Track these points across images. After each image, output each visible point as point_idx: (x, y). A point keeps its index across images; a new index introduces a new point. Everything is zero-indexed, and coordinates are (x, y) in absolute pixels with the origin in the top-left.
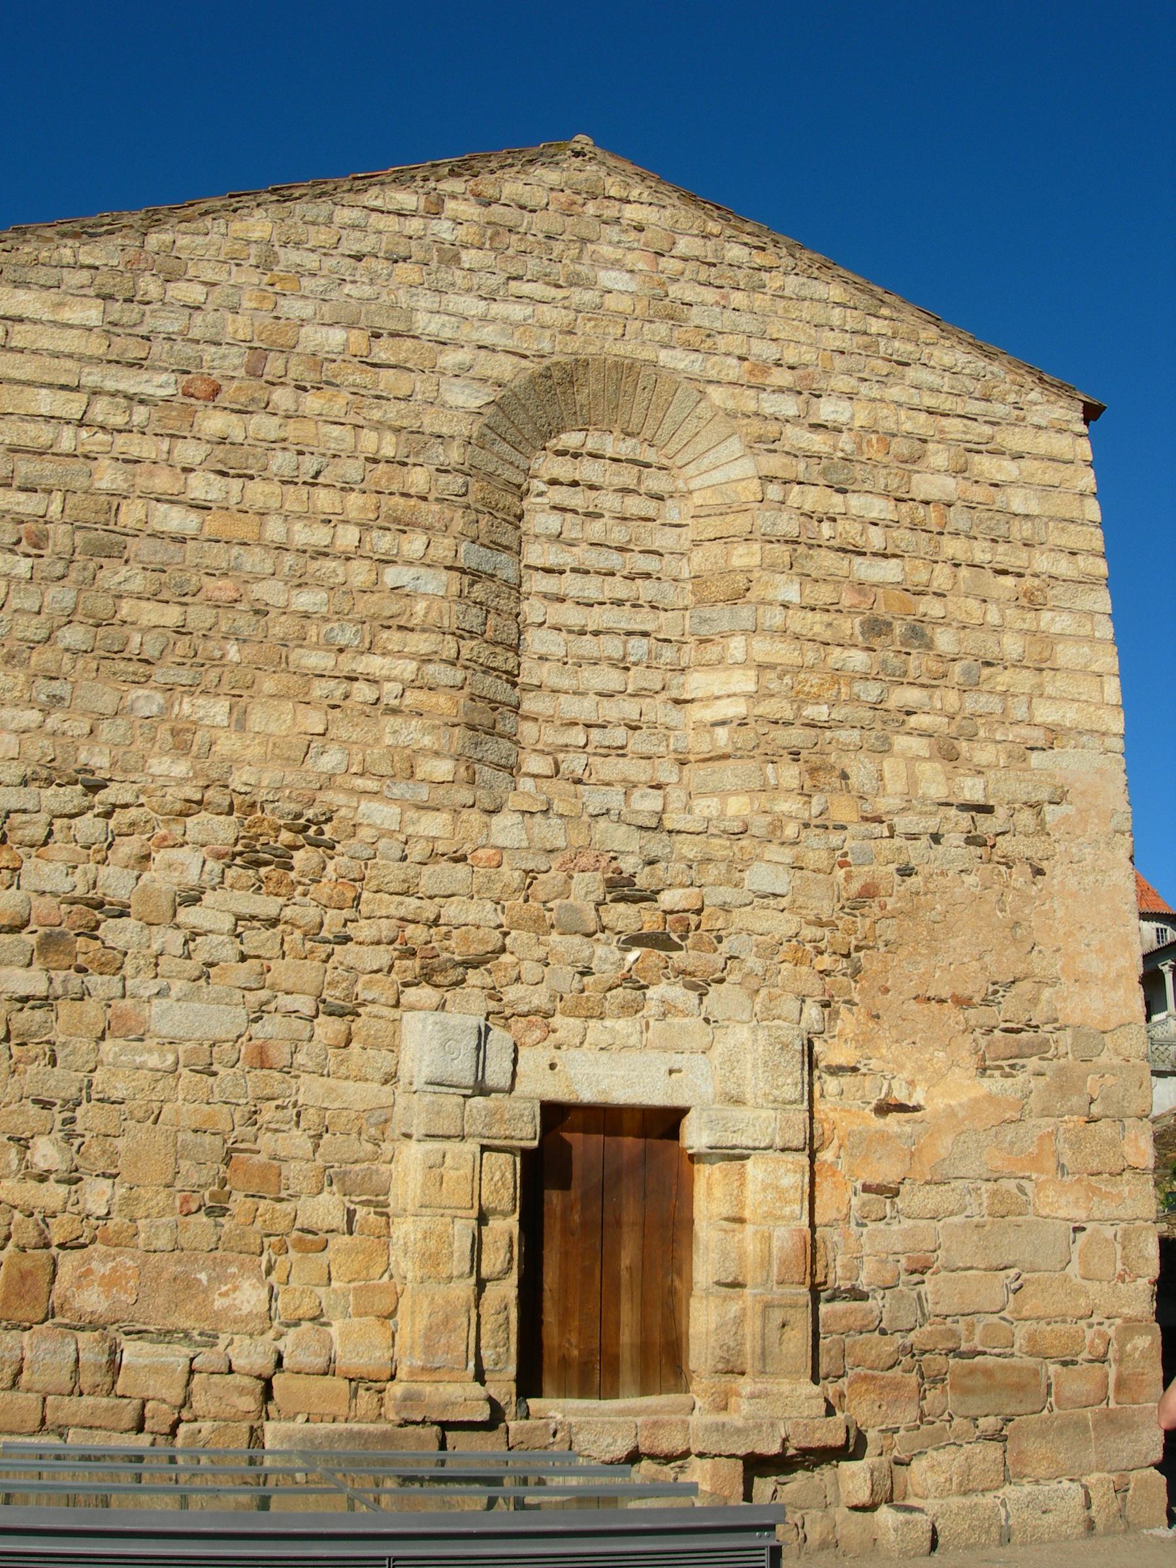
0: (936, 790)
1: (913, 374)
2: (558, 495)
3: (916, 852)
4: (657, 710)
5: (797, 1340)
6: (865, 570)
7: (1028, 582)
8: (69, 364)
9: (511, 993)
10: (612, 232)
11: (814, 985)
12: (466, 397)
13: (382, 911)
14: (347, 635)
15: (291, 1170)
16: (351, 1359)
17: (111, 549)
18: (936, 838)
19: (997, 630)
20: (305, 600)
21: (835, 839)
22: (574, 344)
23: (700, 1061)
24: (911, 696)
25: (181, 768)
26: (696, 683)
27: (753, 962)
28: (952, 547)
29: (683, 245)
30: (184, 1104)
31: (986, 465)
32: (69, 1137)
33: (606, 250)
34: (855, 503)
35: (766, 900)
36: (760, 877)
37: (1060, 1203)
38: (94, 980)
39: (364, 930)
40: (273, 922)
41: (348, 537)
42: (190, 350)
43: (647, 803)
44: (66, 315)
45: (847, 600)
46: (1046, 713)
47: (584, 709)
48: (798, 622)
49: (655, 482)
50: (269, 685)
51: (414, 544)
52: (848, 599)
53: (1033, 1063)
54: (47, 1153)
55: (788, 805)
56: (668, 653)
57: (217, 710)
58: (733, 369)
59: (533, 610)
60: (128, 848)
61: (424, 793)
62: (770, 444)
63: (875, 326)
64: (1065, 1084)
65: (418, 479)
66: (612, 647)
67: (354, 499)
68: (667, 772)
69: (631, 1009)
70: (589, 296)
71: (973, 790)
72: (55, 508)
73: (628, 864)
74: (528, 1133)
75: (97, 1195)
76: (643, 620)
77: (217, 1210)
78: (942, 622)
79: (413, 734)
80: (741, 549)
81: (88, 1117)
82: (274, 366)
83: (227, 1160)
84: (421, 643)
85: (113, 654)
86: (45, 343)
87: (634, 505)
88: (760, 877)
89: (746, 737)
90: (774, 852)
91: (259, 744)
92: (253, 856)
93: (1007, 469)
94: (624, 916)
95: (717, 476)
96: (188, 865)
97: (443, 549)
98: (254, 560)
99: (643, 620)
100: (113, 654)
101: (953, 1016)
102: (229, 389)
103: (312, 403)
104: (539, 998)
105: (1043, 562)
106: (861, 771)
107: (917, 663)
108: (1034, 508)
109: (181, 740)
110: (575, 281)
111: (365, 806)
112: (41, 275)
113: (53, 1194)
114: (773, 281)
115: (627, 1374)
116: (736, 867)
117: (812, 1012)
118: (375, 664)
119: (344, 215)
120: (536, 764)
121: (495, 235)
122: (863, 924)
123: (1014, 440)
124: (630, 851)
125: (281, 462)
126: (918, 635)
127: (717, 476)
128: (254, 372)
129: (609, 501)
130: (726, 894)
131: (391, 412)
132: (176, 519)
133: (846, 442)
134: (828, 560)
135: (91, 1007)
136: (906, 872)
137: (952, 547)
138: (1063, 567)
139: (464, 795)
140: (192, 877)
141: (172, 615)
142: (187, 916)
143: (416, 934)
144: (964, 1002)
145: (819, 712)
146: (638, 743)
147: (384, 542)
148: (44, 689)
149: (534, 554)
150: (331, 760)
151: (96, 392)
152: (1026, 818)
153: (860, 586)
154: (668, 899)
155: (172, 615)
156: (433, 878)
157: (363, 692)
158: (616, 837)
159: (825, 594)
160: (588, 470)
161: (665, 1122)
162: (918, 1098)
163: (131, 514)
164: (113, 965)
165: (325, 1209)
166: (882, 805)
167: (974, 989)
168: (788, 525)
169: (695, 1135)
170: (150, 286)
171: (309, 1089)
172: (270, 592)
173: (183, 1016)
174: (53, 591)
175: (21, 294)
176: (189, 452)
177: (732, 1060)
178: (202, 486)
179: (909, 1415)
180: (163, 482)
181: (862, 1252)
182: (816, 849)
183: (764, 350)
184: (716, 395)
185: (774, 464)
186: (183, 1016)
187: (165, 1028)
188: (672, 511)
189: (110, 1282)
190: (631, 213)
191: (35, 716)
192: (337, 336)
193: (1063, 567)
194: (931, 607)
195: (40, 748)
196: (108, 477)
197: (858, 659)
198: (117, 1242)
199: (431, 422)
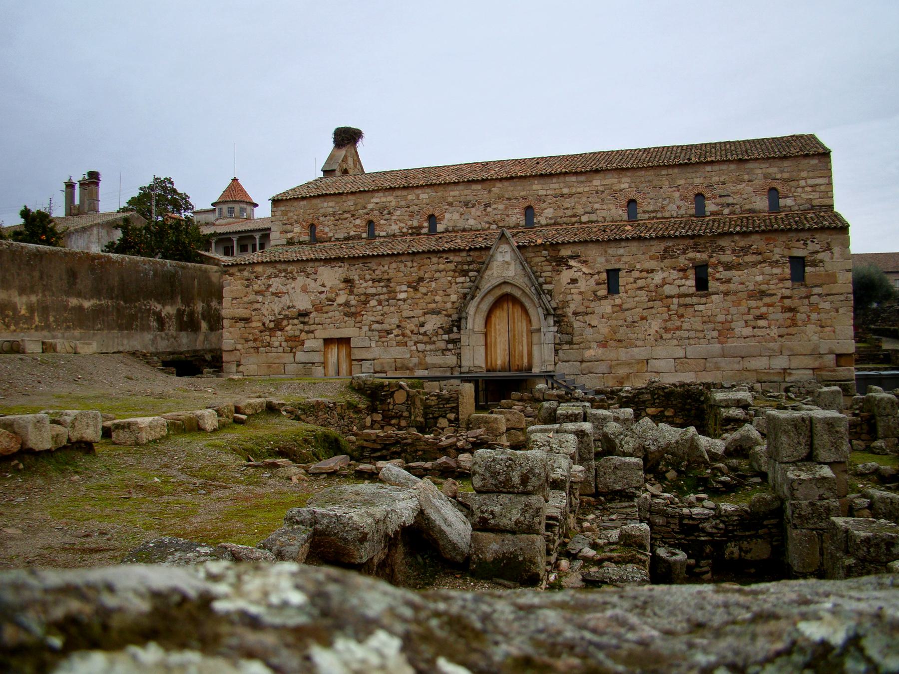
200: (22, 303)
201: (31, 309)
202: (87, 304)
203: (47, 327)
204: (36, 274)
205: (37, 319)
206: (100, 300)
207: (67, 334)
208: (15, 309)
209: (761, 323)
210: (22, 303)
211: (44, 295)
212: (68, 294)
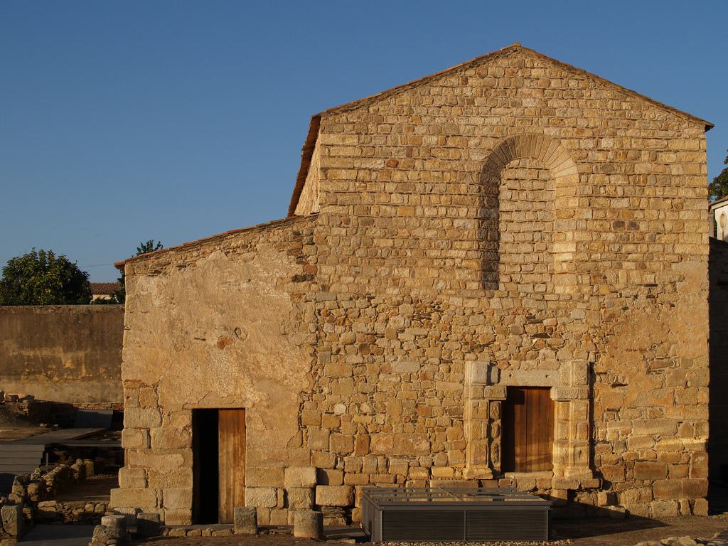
0: (637, 281)
2: (510, 184)
3: (629, 302)
4: (544, 257)
6: (616, 204)
7: (676, 201)
8: (350, 160)
10: (527, 82)
12: (478, 157)
13: (458, 331)
15: (435, 409)
17: (370, 223)
18: (636, 297)
20: (430, 234)
25: (396, 291)
26: (557, 247)
30: (404, 391)
31: (663, 157)
33: (525, 90)
34: (613, 178)
35: (578, 321)
38: (376, 357)
39: (453, 337)
43: (542, 289)
44: (347, 142)
46: (679, 249)
47: (519, 259)
48: (590, 225)
49: (542, 176)
50: (420, 263)
51: (463, 212)
53: (667, 369)
54: (366, 408)
58: (571, 133)
60: (382, 317)
63: (624, 106)
64: (677, 376)
67: (443, 197)
68: (547, 278)
69: (533, 357)
71: (650, 279)
72: (351, 210)
73: (533, 312)
75: (380, 419)
76: (539, 227)
77: (414, 422)
78: (644, 219)
80: (571, 200)
82: (415, 153)
83: (417, 406)
84: (466, 245)
85: (373, 256)
86: (341, 153)
87: (536, 185)
88: (575, 314)
90: (580, 305)
93: (673, 156)
94: (531, 329)
95: (564, 173)
96: (400, 321)
99: (539, 227)
100: (373, 256)
103: (428, 165)
104: (506, 356)
105: (682, 193)
106: (610, 276)
107: (633, 234)
109: (396, 282)
110: (515, 105)
112: (336, 128)
113: (368, 419)
114: (586, 94)
118: (453, 253)
121: (485, 91)
123: (675, 145)
124: (532, 306)
126: (634, 225)
128: (409, 155)
129: (527, 185)
130: (565, 319)
131: (454, 165)
133: (611, 155)
134: (602, 201)
136: (625, 309)
138: (691, 194)
139: (482, 293)
140: (401, 324)
141: (390, 242)
142: (400, 336)
143: (468, 337)
146: (538, 269)
148: (353, 270)
149: (503, 207)
150: (441, 285)
151: (360, 169)
153: (613, 211)
154: (545, 322)
155: (390, 242)
157: (449, 263)
159: (601, 214)
160: (521, 174)
162: (627, 381)
166: (617, 287)
168: (588, 191)
169: (554, 395)
171: (439, 386)
172: (418, 232)
173: (402, 366)
175: (332, 136)
176: (390, 187)
177: (565, 373)
178: (395, 199)
180: (383, 199)
182: (594, 303)
183: (582, 123)
184: (564, 142)
185: (585, 167)
186: (402, 366)
189: (386, 443)
190: (535, 73)
191: (351, 279)
193: (691, 194)
195: (354, 288)
196: (367, 198)
200: (67, 361)
201: (78, 363)
203: (98, 377)
205: (84, 370)
210: (67, 361)
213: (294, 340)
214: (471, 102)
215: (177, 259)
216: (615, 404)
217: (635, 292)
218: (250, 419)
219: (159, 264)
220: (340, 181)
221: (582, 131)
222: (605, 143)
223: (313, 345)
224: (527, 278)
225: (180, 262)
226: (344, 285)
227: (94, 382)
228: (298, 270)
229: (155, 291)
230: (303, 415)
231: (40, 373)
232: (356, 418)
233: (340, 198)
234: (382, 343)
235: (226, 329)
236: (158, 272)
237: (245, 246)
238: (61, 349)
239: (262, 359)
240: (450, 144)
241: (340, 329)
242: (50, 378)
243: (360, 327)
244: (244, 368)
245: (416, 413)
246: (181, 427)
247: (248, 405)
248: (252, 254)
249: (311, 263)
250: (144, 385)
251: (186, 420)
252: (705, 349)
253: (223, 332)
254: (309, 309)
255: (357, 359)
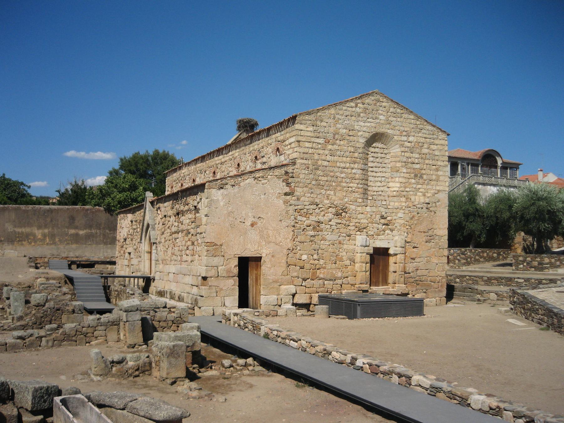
0: (422, 201)
1: (423, 131)
2: (373, 154)
4: (385, 189)
5: (402, 279)
7: (437, 167)
9: (369, 232)
11: (406, 230)
14: (348, 180)
15: (344, 257)
16: (351, 282)
17: (317, 169)
19: (432, 175)
20: (343, 175)
21: (409, 209)
22: (376, 129)
23: (392, 241)
24: (419, 186)
27: (398, 227)
28: (427, 161)
29: (392, 110)
31: (433, 147)
32: (318, 254)
33: (380, 112)
34: (414, 155)
36: (400, 215)
37: (435, 260)
39: (351, 224)
40: (340, 224)
41: (348, 165)
42: (325, 134)
43: (385, 203)
44: (308, 129)
45: (412, 171)
46: (438, 188)
49: (386, 151)
51: (356, 166)
52: (412, 171)
53: (433, 241)
54: (315, 257)
55: (404, 204)
56: (387, 180)
57: (332, 193)
58: (398, 133)
59: (370, 174)
61: (358, 204)
62: (402, 145)
63: (418, 123)
65: (356, 155)
66: (380, 179)
69: (383, 234)
70: (378, 121)
71: (427, 201)
73: (383, 213)
74: (372, 252)
75: (322, 262)
76: (384, 175)
77: (335, 263)
79: (356, 195)
81: (320, 251)
82: (336, 136)
84: (357, 181)
87: (383, 155)
88: (400, 215)
89: (398, 194)
91: (337, 198)
92: (337, 214)
94: (383, 221)
95: (394, 151)
96: (330, 216)
97: (359, 167)
98: (336, 169)
99: (384, 175)
101: (423, 234)
102: (331, 141)
103: (342, 143)
104: (372, 233)
105: (439, 163)
106: (413, 198)
107: (421, 181)
108: (438, 154)
110: (376, 118)
111: (351, 206)
112: (303, 122)
113: (316, 262)
114: (404, 115)
115: (380, 284)
116: (397, 213)
117: (406, 234)
118: (351, 185)
119: (344, 108)
120: (370, 198)
122: (412, 221)
123: (436, 142)
125: (338, 153)
126: (421, 177)
127: (394, 151)
128: (334, 138)
130: (395, 217)
132: (326, 163)
134: (410, 165)
135: (320, 236)
136: (418, 213)
137: (427, 161)
138: (442, 164)
141: (326, 179)
142: (329, 223)
144: (424, 232)
145: (408, 189)
146: (383, 194)
147: (352, 165)
148: (311, 191)
149: (370, 164)
150: (346, 200)
152: (434, 205)
154: (389, 218)
155: (326, 179)
156: (360, 216)
158: (382, 209)
159: (409, 170)
160: (377, 150)
161: (388, 249)
163: (320, 162)
164: (322, 231)
165: (348, 263)
167: (426, 230)
168: (405, 160)
169: (391, 252)
170: (319, 123)
172: (338, 174)
173: (330, 237)
174: (311, 175)
176: (327, 152)
178: (329, 158)
179: (415, 289)
180: (324, 158)
181: (410, 267)
183: (402, 128)
185: (403, 149)
186: (330, 237)
187: (328, 239)
188: (388, 156)
189: (324, 273)
190: (384, 104)
192: (344, 131)
193: (442, 164)
194: (423, 172)
196: (316, 157)
197: (413, 181)
198: (325, 268)
199: (357, 145)
200: (39, 233)
201: (44, 236)
202: (81, 232)
203: (54, 243)
204: (49, 220)
205: (48, 240)
206: (91, 230)
207: (67, 247)
208: (34, 236)
209: (188, 252)
210: (39, 233)
211: (53, 228)
212: (68, 228)
213: (284, 224)
214: (359, 115)
215: (232, 182)
216: (414, 256)
217: (422, 206)
218: (265, 262)
219: (222, 184)
220: (305, 147)
221: (401, 132)
222: (411, 139)
223: (294, 226)
224: (380, 198)
225: (233, 183)
226: (306, 200)
227: (53, 246)
228: (287, 190)
229: (220, 198)
230: (288, 260)
231: (25, 241)
232: (312, 262)
233: (306, 156)
234: (322, 226)
235: (254, 217)
236: (222, 188)
237: (263, 177)
238: (36, 229)
239: (270, 233)
240: (351, 134)
241: (304, 219)
242: (30, 243)
243: (313, 218)
244: (262, 237)
245: (337, 259)
246: (233, 266)
247: (264, 255)
248: (266, 181)
249: (293, 187)
250: (216, 245)
251: (236, 262)
252: (446, 232)
253: (253, 219)
254: (291, 208)
255: (312, 233)
